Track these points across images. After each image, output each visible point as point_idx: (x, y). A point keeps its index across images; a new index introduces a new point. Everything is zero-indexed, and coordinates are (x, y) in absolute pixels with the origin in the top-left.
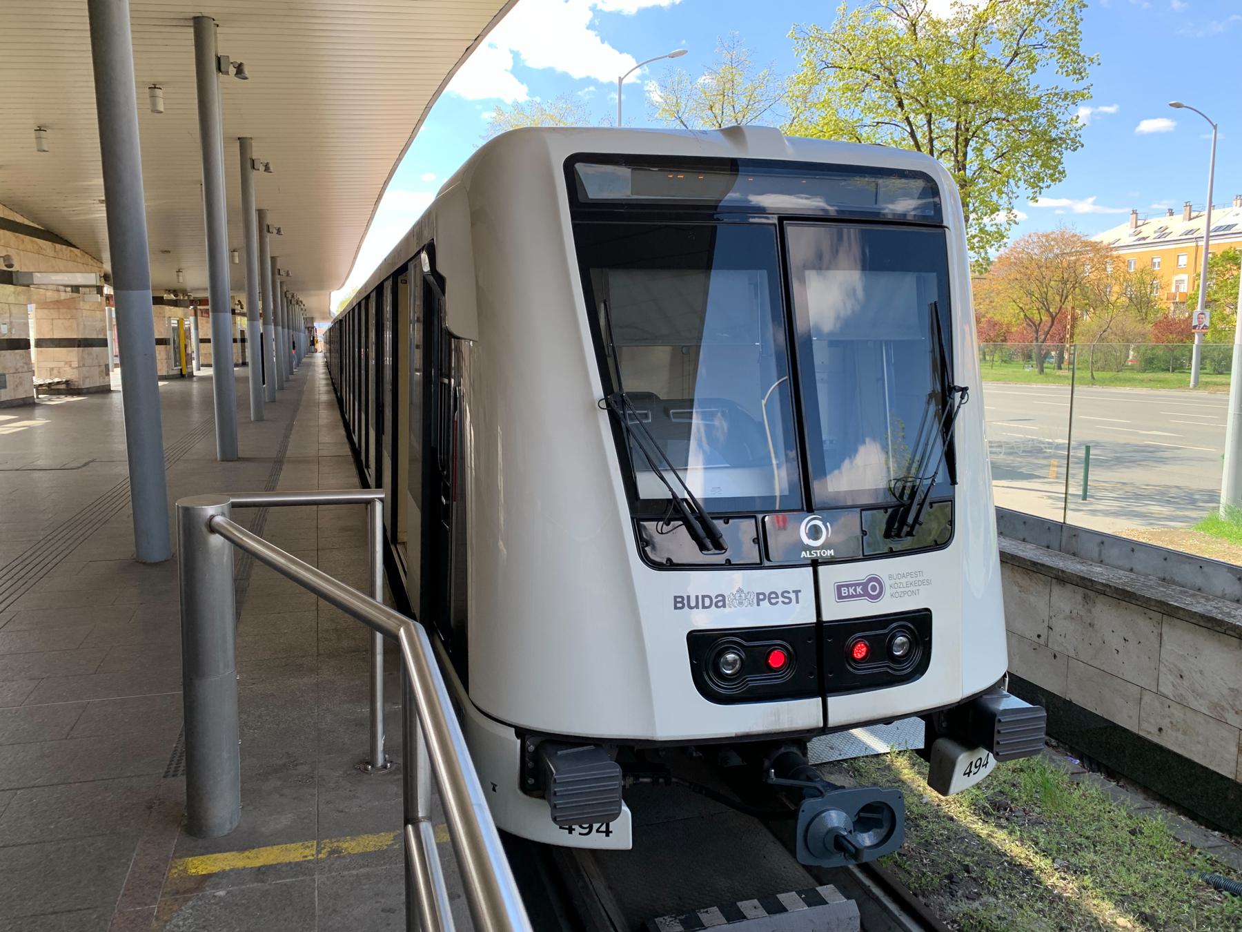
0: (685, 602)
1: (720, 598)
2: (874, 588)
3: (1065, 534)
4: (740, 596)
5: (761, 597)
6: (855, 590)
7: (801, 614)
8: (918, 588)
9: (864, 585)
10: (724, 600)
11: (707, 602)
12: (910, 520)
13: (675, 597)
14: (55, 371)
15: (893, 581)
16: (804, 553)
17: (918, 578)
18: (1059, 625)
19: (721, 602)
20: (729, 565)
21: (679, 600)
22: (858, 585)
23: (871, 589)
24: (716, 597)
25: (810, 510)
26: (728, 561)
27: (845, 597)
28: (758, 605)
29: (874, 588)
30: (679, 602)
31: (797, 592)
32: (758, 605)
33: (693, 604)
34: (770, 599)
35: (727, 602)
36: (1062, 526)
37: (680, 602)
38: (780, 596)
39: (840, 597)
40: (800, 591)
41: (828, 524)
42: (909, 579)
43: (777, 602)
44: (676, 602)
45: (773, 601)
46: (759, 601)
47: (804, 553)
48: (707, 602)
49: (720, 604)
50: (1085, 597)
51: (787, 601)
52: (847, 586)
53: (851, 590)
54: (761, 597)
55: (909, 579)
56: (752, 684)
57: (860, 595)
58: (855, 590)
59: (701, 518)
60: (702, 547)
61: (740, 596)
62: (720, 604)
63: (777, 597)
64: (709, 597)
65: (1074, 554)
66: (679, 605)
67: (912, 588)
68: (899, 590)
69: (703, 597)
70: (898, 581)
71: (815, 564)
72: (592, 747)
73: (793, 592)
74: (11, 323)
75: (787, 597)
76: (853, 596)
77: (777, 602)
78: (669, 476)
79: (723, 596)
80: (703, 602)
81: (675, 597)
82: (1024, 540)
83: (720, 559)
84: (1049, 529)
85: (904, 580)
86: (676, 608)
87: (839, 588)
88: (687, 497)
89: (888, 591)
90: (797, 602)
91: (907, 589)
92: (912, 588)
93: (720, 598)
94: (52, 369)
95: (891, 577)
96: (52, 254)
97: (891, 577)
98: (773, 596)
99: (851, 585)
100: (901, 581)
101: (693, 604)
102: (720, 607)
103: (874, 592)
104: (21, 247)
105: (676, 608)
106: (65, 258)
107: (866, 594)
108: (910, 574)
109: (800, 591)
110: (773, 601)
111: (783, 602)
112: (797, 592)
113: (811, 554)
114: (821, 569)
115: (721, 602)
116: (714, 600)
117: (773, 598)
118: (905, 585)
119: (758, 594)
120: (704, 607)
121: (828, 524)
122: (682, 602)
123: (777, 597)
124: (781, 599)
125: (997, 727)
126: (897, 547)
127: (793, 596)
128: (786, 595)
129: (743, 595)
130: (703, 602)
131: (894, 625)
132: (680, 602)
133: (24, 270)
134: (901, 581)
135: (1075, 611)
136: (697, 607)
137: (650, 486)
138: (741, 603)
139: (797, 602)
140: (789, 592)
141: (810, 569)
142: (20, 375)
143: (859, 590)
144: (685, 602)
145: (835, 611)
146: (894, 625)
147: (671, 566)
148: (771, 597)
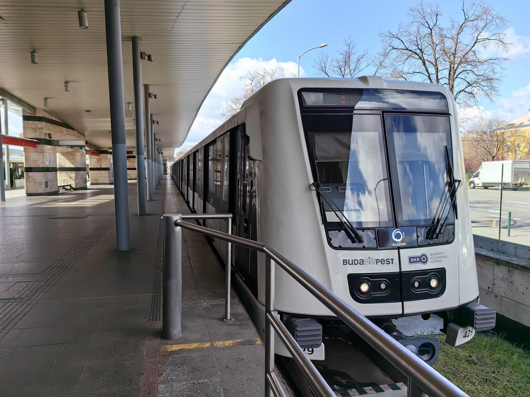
0: (348, 262)
1: (361, 261)
2: (424, 259)
3: (500, 244)
4: (370, 260)
5: (378, 261)
6: (416, 259)
7: (393, 269)
8: (441, 259)
9: (420, 257)
10: (363, 262)
11: (356, 262)
12: (437, 232)
13: (344, 260)
14: (66, 181)
15: (431, 256)
16: (393, 244)
17: (442, 255)
18: (497, 282)
19: (362, 262)
20: (364, 248)
21: (345, 261)
22: (418, 257)
23: (423, 259)
24: (360, 260)
25: (397, 227)
26: (364, 246)
27: (412, 262)
28: (377, 264)
29: (424, 259)
30: (345, 262)
31: (392, 260)
32: (377, 264)
33: (351, 263)
34: (381, 262)
35: (364, 262)
36: (498, 241)
37: (345, 262)
38: (385, 261)
39: (410, 262)
40: (393, 259)
41: (403, 233)
42: (438, 255)
44: (344, 262)
45: (383, 263)
47: (393, 244)
48: (356, 262)
49: (361, 263)
50: (509, 271)
51: (388, 263)
52: (413, 258)
53: (415, 260)
54: (378, 261)
55: (438, 255)
56: (373, 295)
57: (418, 262)
58: (416, 259)
59: (352, 229)
60: (353, 242)
61: (370, 260)
62: (361, 263)
63: (384, 261)
65: (504, 253)
66: (345, 263)
67: (440, 259)
68: (434, 260)
69: (355, 260)
70: (433, 256)
71: (399, 248)
72: (310, 319)
73: (391, 259)
74: (50, 161)
75: (389, 262)
76: (415, 262)
77: (384, 263)
78: (338, 213)
80: (354, 262)
81: (344, 260)
82: (481, 247)
83: (361, 245)
84: (493, 242)
85: (436, 256)
86: (344, 264)
87: (410, 258)
88: (346, 221)
89: (429, 260)
90: (392, 263)
91: (437, 260)
92: (439, 259)
93: (361, 261)
94: (64, 180)
95: (431, 254)
96: (66, 133)
97: (431, 254)
98: (383, 260)
99: (415, 257)
100: (435, 256)
101: (351, 263)
102: (361, 264)
103: (424, 260)
104: (55, 130)
105: (344, 264)
106: (71, 134)
107: (421, 261)
108: (438, 253)
109: (393, 259)
110: (383, 263)
111: (387, 263)
112: (392, 260)
113: (396, 245)
114: (401, 250)
115: (362, 262)
116: (359, 262)
117: (383, 261)
118: (436, 258)
119: (377, 260)
120: (355, 264)
121: (403, 233)
122: (346, 262)
123: (384, 261)
124: (386, 262)
125: (475, 317)
126: (431, 242)
127: (391, 261)
128: (388, 260)
129: (371, 260)
130: (354, 262)
131: (432, 273)
132: (345, 262)
133: (56, 139)
134: (435, 256)
135: (504, 277)
136: (352, 264)
137: (331, 217)
138: (370, 263)
139: (392, 263)
141: (397, 250)
142: (53, 182)
143: (418, 259)
144: (348, 262)
145: (407, 267)
146: (432, 273)
147: (340, 248)
148: (382, 261)
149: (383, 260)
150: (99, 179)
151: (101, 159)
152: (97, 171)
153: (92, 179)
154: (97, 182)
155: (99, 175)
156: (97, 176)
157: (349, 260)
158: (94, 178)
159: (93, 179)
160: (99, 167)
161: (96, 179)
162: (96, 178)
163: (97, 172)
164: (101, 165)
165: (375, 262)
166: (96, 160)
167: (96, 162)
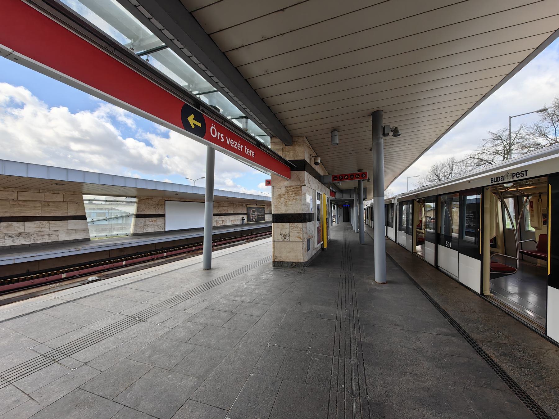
1: (502, 177)
31: (526, 171)
38: (520, 174)
40: (527, 170)
43: (519, 176)
44: (491, 181)
45: (518, 176)
46: (513, 176)
49: (502, 179)
51: (522, 175)
64: (499, 177)
66: (492, 181)
69: (498, 177)
73: (525, 171)
77: (519, 176)
79: (503, 176)
93: (502, 177)
98: (518, 174)
109: (527, 170)
112: (526, 171)
117: (518, 175)
119: (513, 174)
122: (493, 180)
123: (519, 174)
124: (520, 175)
127: (524, 173)
140: (523, 172)
149: (518, 174)
157: (494, 178)
165: (512, 176)
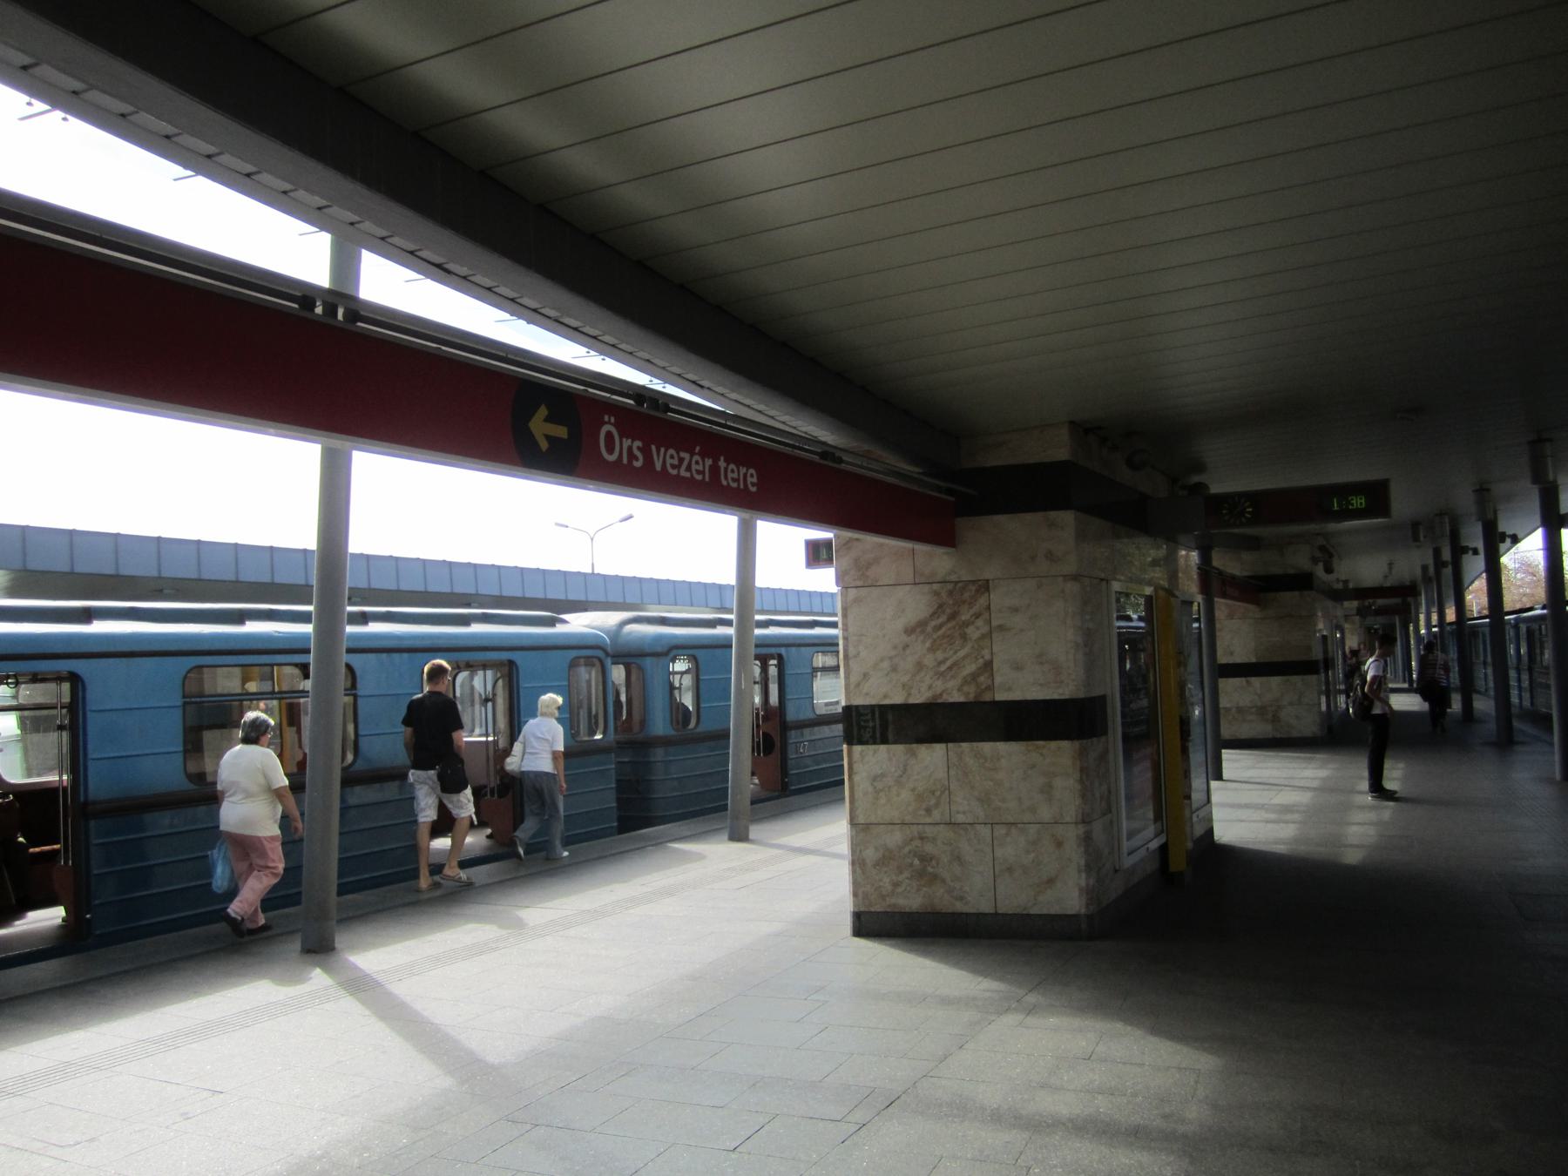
150: (958, 859)
151: (985, 587)
152: (939, 748)
153: (870, 854)
154: (944, 901)
155: (964, 806)
156: (937, 815)
158: (894, 838)
159: (886, 858)
160: (957, 697)
161: (926, 859)
162: (929, 848)
163: (933, 757)
164: (988, 665)
166: (916, 605)
167: (922, 624)
